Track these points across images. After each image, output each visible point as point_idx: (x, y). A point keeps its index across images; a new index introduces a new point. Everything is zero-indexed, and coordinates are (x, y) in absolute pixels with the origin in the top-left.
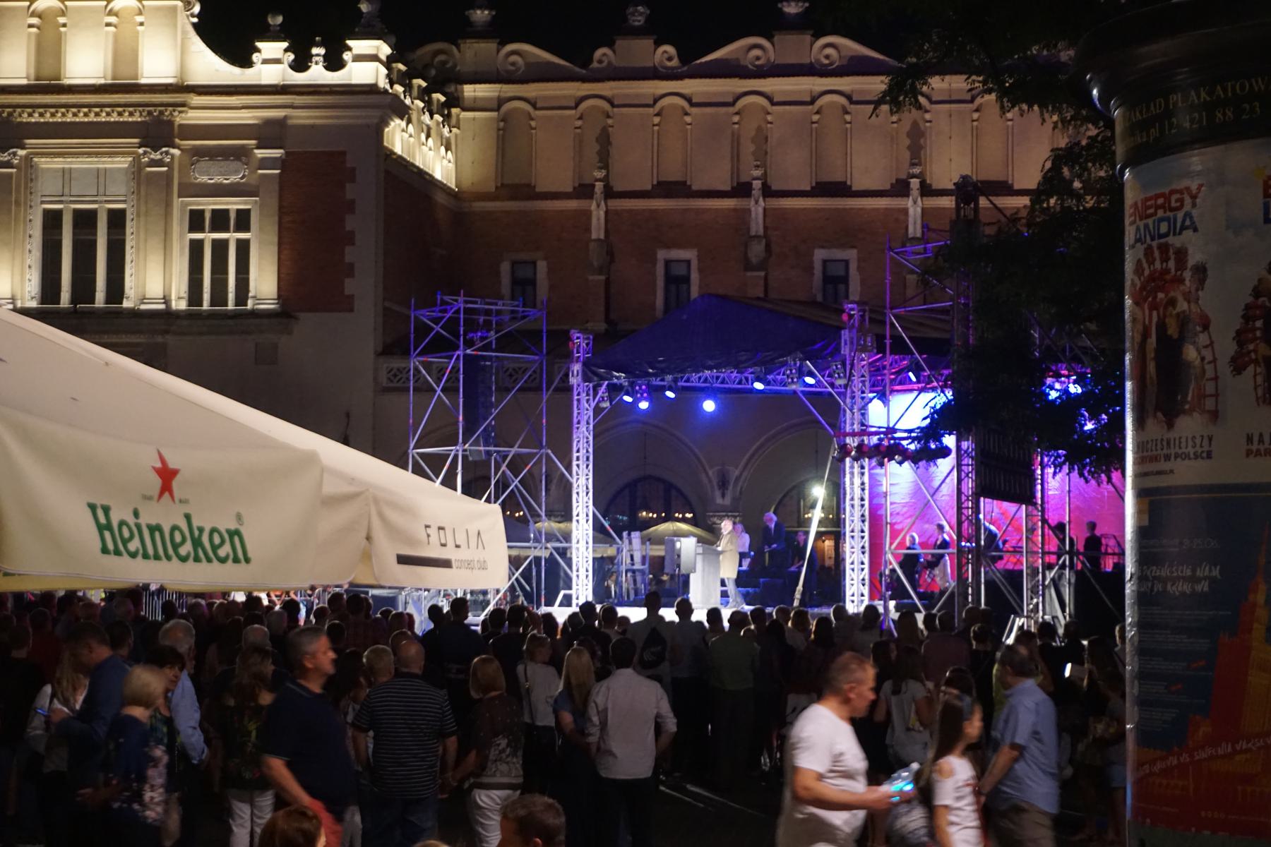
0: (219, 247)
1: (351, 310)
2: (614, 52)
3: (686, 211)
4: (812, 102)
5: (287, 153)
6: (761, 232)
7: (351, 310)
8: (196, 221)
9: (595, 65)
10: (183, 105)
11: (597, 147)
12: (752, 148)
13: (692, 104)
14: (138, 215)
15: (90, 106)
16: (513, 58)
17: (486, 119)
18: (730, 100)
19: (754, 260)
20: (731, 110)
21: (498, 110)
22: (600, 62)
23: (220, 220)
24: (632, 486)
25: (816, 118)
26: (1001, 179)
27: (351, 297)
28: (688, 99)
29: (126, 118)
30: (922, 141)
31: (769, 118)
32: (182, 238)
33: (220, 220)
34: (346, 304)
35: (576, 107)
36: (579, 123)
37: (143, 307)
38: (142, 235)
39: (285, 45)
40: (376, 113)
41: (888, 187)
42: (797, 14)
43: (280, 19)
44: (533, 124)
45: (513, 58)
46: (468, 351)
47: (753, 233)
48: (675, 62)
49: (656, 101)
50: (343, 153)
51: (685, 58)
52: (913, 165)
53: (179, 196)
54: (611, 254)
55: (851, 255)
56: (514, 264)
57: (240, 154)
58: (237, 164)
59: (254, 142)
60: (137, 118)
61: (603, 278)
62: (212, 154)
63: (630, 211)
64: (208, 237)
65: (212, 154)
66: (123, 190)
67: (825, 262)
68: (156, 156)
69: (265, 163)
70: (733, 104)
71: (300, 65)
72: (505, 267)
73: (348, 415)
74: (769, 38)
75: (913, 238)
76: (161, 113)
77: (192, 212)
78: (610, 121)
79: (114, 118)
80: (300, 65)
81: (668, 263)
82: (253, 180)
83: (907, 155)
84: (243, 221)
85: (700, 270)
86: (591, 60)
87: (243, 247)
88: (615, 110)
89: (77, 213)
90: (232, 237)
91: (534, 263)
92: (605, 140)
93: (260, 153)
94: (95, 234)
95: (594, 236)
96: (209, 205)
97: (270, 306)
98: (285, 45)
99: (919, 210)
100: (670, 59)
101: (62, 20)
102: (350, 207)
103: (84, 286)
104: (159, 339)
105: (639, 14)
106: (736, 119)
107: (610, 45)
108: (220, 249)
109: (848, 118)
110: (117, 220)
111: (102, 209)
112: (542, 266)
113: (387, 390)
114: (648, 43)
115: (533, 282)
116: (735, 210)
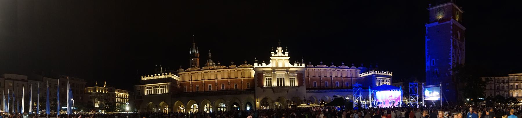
0: (292, 81)
23: (292, 79)
34: (303, 86)
57: (294, 73)
69: (296, 74)
87: (294, 81)
89: (280, 78)
90: (293, 80)
96: (291, 77)
97: (297, 86)
110: (284, 78)
111: (282, 77)
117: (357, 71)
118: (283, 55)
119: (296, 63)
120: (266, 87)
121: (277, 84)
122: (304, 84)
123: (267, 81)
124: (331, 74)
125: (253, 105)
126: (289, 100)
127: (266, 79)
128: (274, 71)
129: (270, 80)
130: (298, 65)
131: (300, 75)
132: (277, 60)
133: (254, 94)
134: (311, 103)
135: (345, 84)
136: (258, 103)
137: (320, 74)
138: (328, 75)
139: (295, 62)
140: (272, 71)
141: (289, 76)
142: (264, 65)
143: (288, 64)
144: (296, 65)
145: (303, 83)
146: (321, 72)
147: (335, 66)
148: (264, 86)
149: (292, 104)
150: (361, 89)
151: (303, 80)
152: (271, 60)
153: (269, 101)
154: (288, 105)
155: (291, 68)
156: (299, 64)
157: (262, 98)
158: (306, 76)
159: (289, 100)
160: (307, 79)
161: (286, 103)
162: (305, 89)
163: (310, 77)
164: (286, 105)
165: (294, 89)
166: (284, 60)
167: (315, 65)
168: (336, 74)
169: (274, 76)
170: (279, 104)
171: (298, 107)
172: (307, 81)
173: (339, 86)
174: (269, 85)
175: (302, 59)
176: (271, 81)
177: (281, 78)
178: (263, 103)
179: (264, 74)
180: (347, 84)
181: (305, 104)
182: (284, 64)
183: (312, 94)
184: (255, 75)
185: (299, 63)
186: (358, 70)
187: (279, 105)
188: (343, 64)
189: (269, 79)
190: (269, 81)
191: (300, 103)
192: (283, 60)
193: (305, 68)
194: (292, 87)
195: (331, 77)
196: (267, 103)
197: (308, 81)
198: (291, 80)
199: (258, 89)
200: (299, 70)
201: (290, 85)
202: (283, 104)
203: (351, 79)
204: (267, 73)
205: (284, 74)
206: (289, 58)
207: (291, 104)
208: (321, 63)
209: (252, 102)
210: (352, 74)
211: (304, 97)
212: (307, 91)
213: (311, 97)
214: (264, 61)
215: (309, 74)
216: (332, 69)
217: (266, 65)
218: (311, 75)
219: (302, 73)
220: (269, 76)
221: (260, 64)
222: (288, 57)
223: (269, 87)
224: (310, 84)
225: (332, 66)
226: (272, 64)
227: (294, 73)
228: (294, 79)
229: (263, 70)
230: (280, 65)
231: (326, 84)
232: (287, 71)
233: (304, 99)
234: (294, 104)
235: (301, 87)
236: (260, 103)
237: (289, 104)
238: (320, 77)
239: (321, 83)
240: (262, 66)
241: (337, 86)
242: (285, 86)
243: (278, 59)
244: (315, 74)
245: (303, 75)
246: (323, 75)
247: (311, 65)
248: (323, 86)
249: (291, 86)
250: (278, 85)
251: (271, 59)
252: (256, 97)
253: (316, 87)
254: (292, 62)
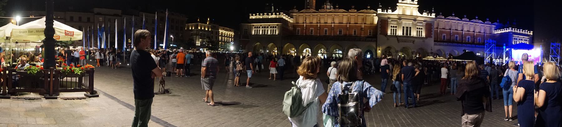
0: (419, 31)
23: (420, 29)
33: (420, 29)
34: (432, 37)
57: (422, 23)
69: (424, 24)
87: (422, 31)
90: (421, 30)
93: (424, 23)
96: (419, 27)
97: (424, 37)
103: (407, 34)
110: (410, 28)
117: (492, 27)
118: (412, 3)
119: (425, 12)
120: (390, 35)
121: (402, 33)
122: (433, 36)
123: (391, 29)
124: (462, 27)
125: (374, 54)
126: (414, 51)
127: (390, 27)
128: (400, 19)
129: (395, 28)
130: (428, 15)
131: (429, 26)
132: (404, 7)
133: (376, 41)
134: (438, 56)
135: (477, 40)
136: (379, 52)
137: (451, 27)
138: (460, 28)
139: (425, 11)
140: (397, 19)
141: (416, 25)
142: (390, 12)
143: (416, 13)
144: (425, 14)
146: (453, 25)
147: (468, 20)
148: (388, 35)
149: (418, 56)
150: (494, 46)
151: (432, 31)
152: (397, 7)
153: (392, 51)
154: (412, 57)
155: (419, 17)
156: (429, 14)
157: (384, 47)
158: (435, 27)
159: (414, 51)
160: (436, 30)
161: (411, 53)
162: (433, 41)
163: (440, 29)
164: (411, 56)
165: (421, 40)
166: (413, 8)
167: (446, 16)
168: (469, 28)
169: (399, 24)
170: (403, 54)
171: (424, 59)
172: (436, 33)
173: (470, 41)
174: (393, 34)
175: (433, 9)
176: (396, 29)
177: (408, 27)
178: (386, 52)
179: (389, 21)
180: (479, 40)
181: (431, 57)
182: (412, 13)
183: (440, 46)
184: (378, 22)
185: (429, 12)
186: (493, 26)
187: (403, 56)
188: (477, 18)
189: (394, 27)
190: (394, 29)
191: (427, 55)
192: (411, 8)
193: (435, 18)
194: (419, 38)
195: (462, 30)
196: (390, 52)
197: (437, 34)
198: (418, 30)
199: (380, 37)
200: (428, 20)
201: (417, 36)
202: (408, 55)
203: (484, 35)
204: (392, 20)
205: (411, 22)
206: (418, 6)
207: (416, 55)
208: (453, 15)
209: (373, 51)
210: (486, 30)
211: (432, 50)
212: (435, 44)
213: (439, 50)
214: (390, 8)
215: (438, 26)
216: (464, 22)
217: (392, 12)
218: (441, 26)
219: (431, 24)
220: (394, 24)
221: (385, 11)
222: (417, 4)
223: (393, 36)
224: (439, 36)
225: (465, 19)
226: (398, 11)
227: (422, 23)
228: (422, 29)
229: (388, 17)
230: (408, 13)
231: (457, 38)
232: (415, 20)
233: (431, 51)
234: (419, 55)
235: (428, 38)
236: (382, 52)
237: (414, 56)
238: (450, 29)
239: (451, 36)
240: (387, 12)
241: (468, 41)
242: (412, 36)
243: (406, 7)
244: (445, 26)
245: (432, 26)
246: (454, 28)
247: (442, 16)
248: (453, 40)
249: (418, 36)
250: (403, 34)
251: (398, 6)
252: (378, 45)
253: (445, 40)
254: (421, 11)
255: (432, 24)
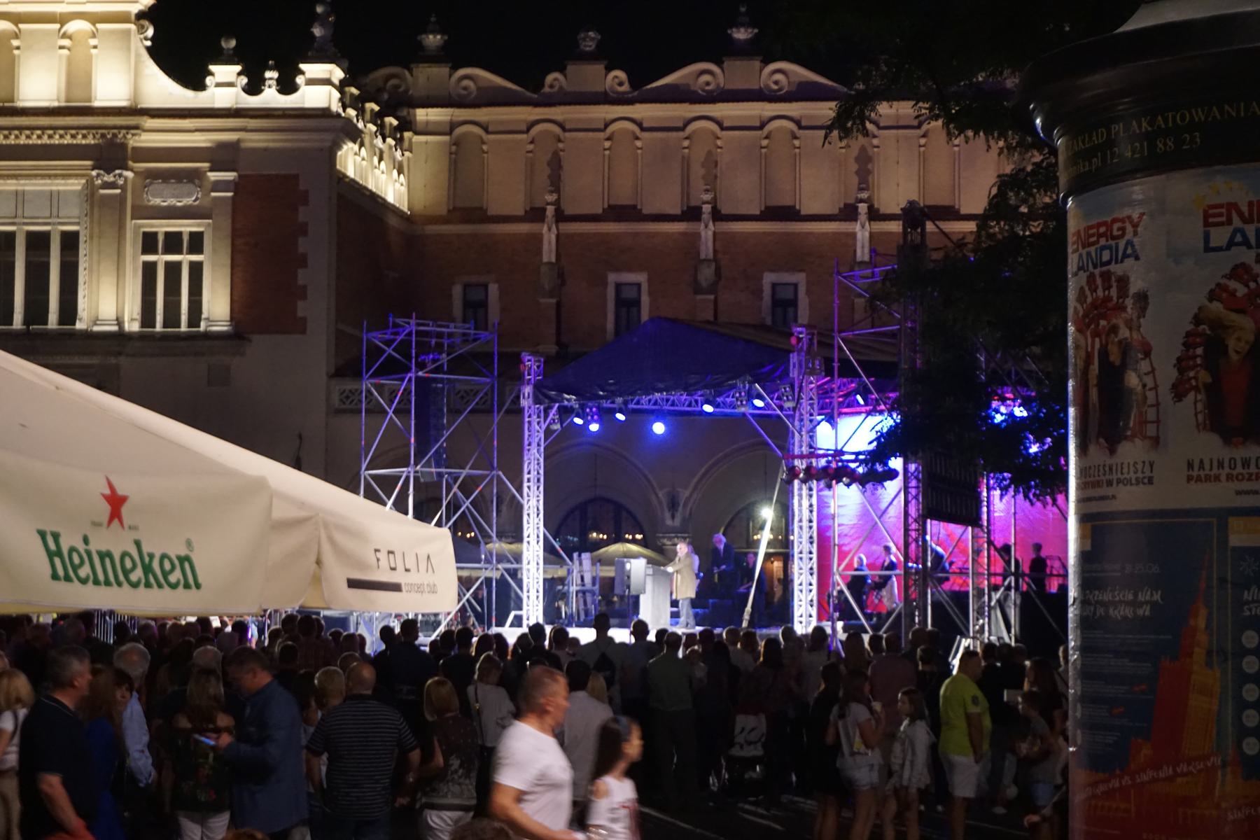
0: (174, 269)
1: (304, 332)
2: (565, 76)
3: (636, 234)
4: (761, 127)
5: (240, 176)
6: (711, 256)
7: (304, 332)
8: (149, 243)
9: (546, 89)
10: (137, 127)
11: (548, 171)
12: (702, 172)
13: (643, 129)
14: (91, 237)
15: (43, 128)
16: (465, 83)
17: (438, 143)
18: (680, 124)
19: (704, 284)
20: (681, 134)
21: (450, 133)
22: (551, 86)
24: (582, 508)
25: (765, 143)
26: (946, 203)
27: (304, 320)
28: (639, 124)
29: (79, 140)
30: (870, 166)
31: (719, 143)
32: (135, 260)
33: (173, 245)
34: (298, 326)
35: (528, 131)
36: (531, 147)
37: (96, 329)
38: (95, 257)
39: (238, 68)
40: (329, 137)
41: (836, 211)
42: (746, 41)
43: (233, 43)
44: (485, 147)
45: (465, 83)
46: (420, 374)
47: (703, 256)
48: (626, 87)
49: (607, 126)
50: (296, 177)
51: (637, 81)
52: (861, 190)
53: (133, 218)
54: (561, 275)
55: (800, 278)
56: (466, 286)
57: (193, 177)
58: (191, 186)
59: (206, 165)
60: (90, 141)
61: (554, 301)
62: (165, 176)
63: (581, 235)
64: (161, 259)
65: (165, 176)
66: (76, 212)
67: (774, 286)
68: (109, 178)
69: (218, 186)
70: (683, 129)
71: (254, 88)
72: (457, 291)
73: (300, 437)
74: (719, 63)
75: (862, 263)
76: (115, 135)
77: (145, 234)
78: (561, 145)
79: (67, 140)
80: (254, 88)
81: (618, 286)
82: (206, 202)
83: (855, 180)
84: (196, 243)
85: (650, 294)
86: (543, 86)
87: (196, 269)
88: (567, 134)
89: (30, 235)
90: (185, 259)
91: (486, 287)
92: (556, 164)
93: (213, 176)
94: (48, 256)
95: (545, 259)
96: (162, 227)
98: (238, 68)
99: (867, 234)
100: (621, 84)
101: (15, 43)
102: (304, 230)
104: (113, 360)
105: (590, 40)
106: (686, 143)
107: (562, 70)
108: (173, 270)
109: (797, 143)
110: (70, 242)
111: (56, 231)
112: (493, 289)
113: (339, 412)
114: (599, 68)
115: (483, 304)
116: (684, 234)
145: (302, 293)
255: (302, 187)
